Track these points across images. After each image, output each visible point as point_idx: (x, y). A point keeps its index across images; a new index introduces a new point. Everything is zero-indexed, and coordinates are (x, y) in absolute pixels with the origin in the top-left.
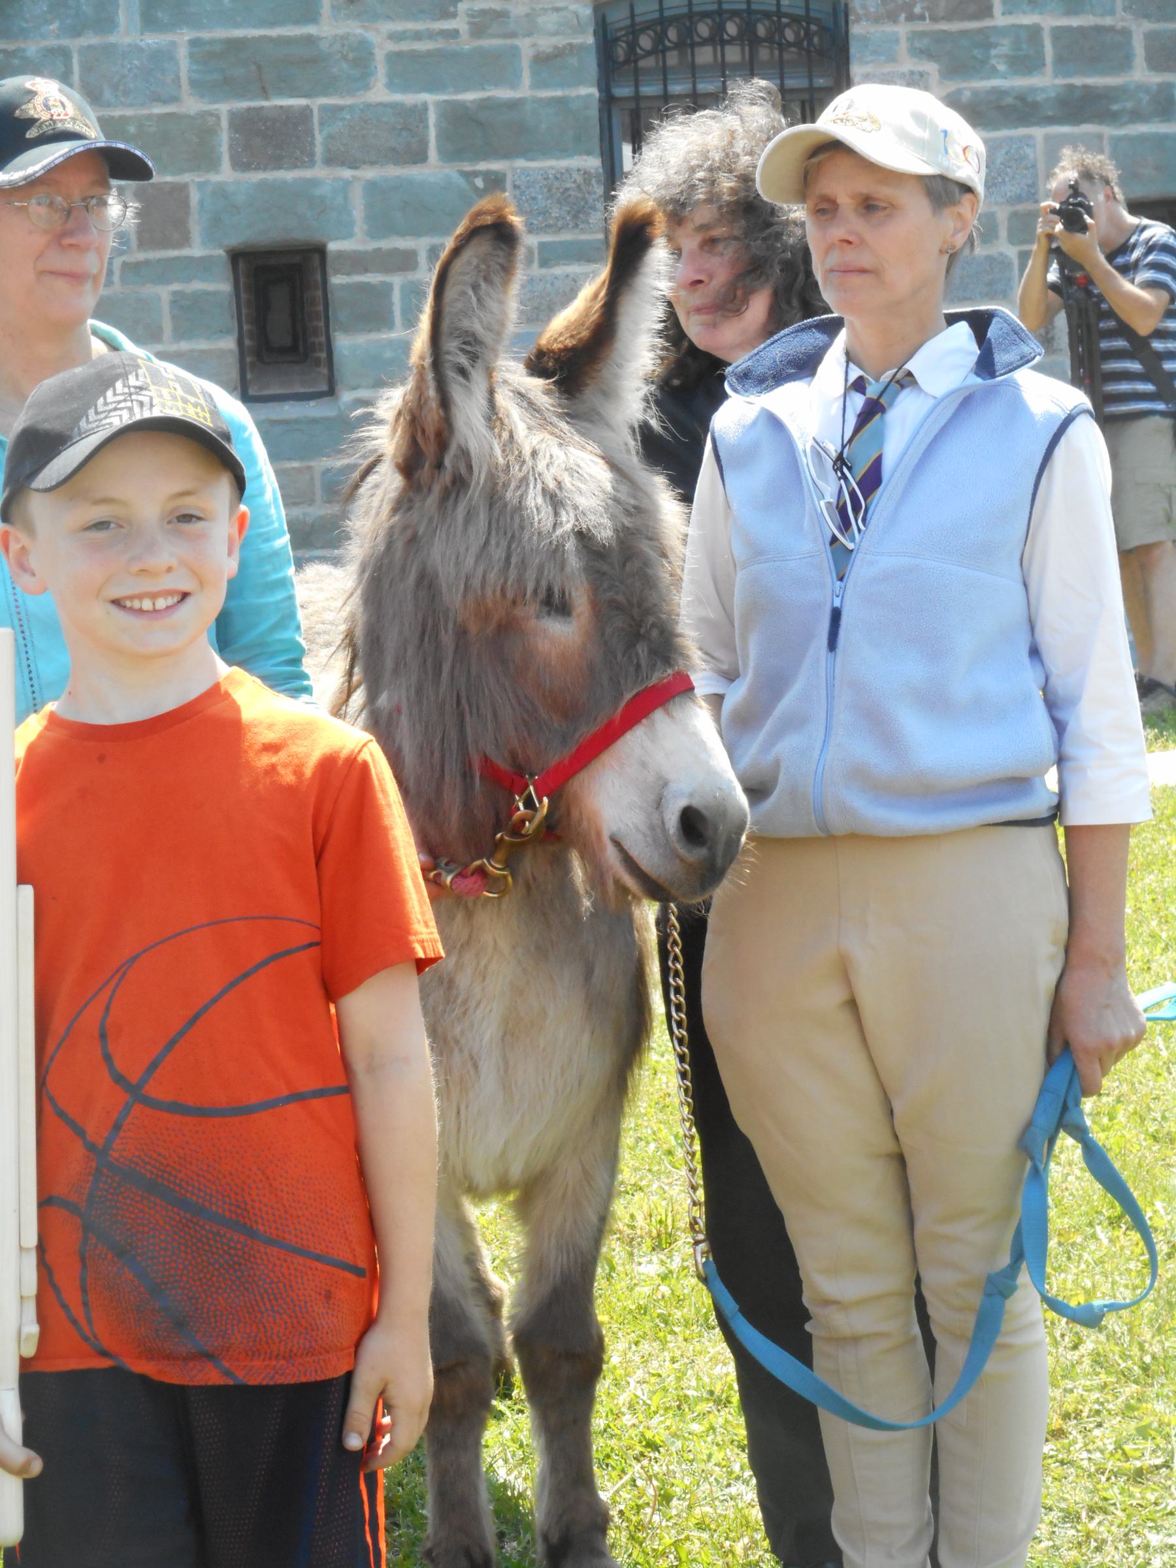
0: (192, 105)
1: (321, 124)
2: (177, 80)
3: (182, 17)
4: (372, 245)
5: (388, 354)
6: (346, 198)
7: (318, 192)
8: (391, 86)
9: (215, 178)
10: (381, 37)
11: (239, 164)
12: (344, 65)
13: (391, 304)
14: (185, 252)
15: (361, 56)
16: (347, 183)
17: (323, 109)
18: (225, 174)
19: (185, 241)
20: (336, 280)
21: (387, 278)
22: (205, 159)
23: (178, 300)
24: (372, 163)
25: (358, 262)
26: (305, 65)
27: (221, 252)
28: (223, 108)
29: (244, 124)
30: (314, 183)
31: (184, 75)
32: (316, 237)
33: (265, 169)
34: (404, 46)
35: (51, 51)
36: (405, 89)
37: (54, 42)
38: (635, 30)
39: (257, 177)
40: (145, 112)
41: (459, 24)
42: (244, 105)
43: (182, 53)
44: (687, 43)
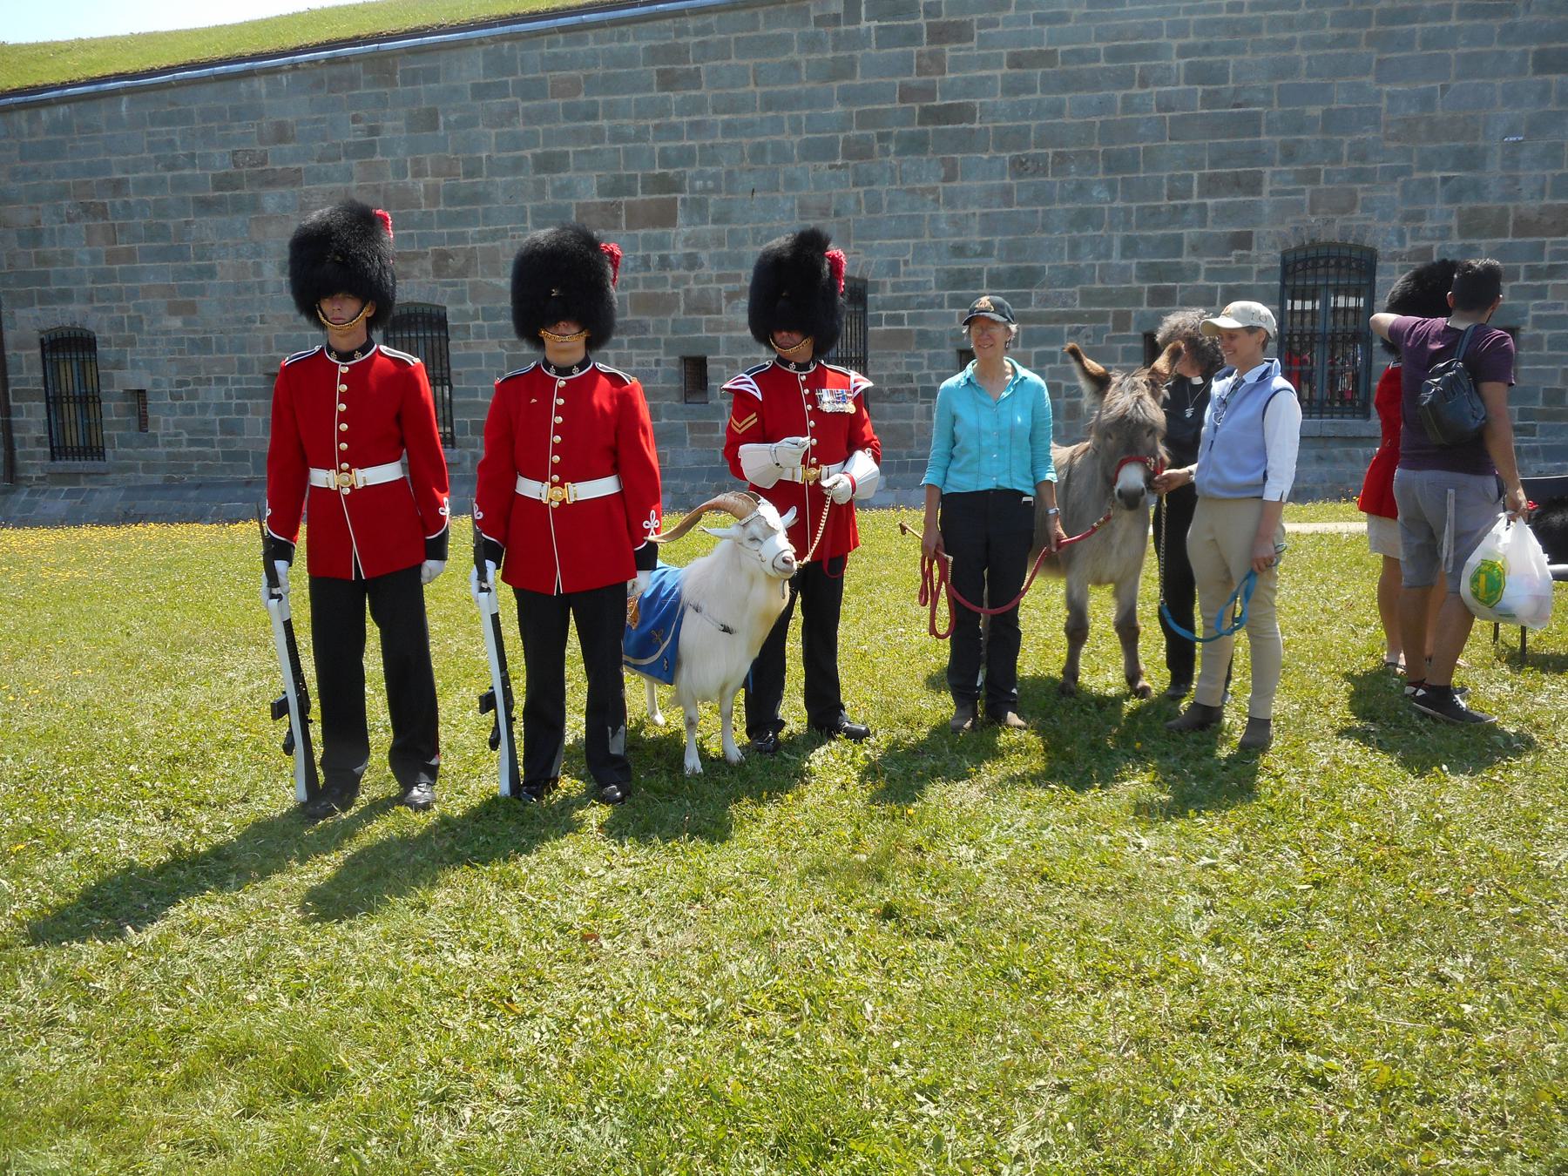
0: (1135, 284)
3: (1135, 254)
8: (1206, 279)
10: (1203, 263)
11: (1150, 304)
15: (1196, 270)
18: (1145, 308)
19: (1128, 329)
22: (1138, 303)
26: (1176, 272)
28: (1146, 286)
29: (1152, 291)
38: (1296, 262)
41: (1232, 259)
44: (1315, 267)
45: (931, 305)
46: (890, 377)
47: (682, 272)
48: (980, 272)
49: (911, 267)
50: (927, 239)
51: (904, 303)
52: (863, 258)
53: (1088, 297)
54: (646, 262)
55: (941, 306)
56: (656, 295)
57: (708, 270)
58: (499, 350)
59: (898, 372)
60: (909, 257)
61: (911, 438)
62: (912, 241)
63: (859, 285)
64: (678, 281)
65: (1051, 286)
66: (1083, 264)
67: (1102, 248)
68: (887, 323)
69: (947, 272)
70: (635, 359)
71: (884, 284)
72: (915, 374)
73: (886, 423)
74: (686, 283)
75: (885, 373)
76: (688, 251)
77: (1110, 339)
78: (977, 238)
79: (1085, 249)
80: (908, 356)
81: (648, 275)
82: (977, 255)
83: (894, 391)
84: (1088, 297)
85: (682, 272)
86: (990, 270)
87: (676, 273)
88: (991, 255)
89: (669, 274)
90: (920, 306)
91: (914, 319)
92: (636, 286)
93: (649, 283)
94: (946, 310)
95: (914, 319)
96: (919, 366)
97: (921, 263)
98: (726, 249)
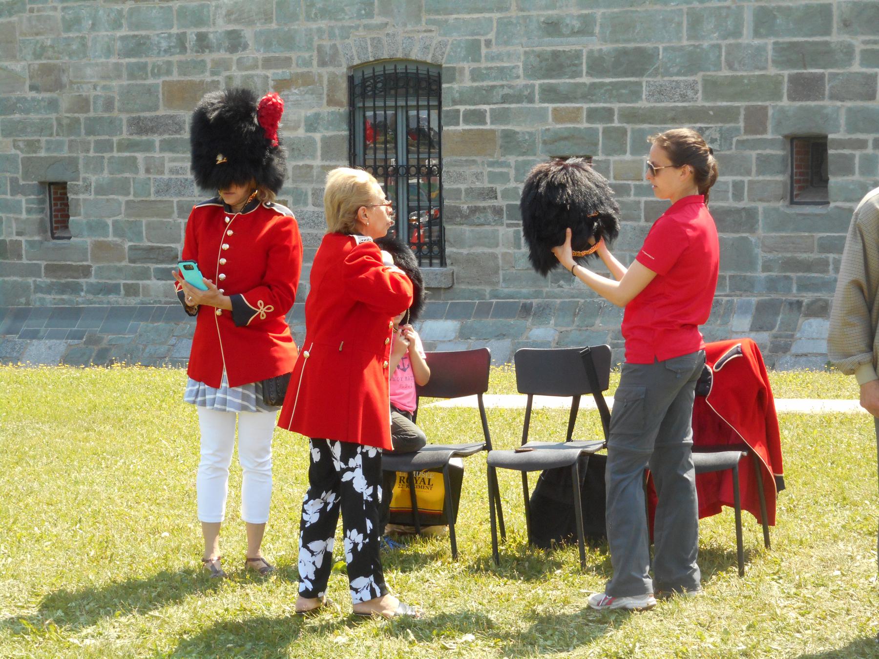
0: (772, 71)
1: (829, 81)
2: (767, 60)
3: (771, 32)
4: (848, 136)
5: (851, 187)
6: (838, 115)
7: (825, 111)
8: (862, 64)
9: (780, 104)
10: (858, 42)
11: (791, 98)
12: (841, 55)
13: (854, 164)
14: (764, 136)
15: (849, 52)
16: (839, 108)
17: (830, 74)
18: (785, 102)
19: (765, 131)
20: (831, 152)
21: (853, 152)
23: (759, 158)
24: (850, 99)
25: (841, 144)
26: (823, 54)
27: (780, 137)
28: (786, 73)
29: (793, 80)
30: (823, 107)
31: (770, 57)
32: (823, 132)
33: (802, 100)
34: (869, 47)
35: (713, 46)
36: (868, 66)
37: (715, 42)
39: (798, 104)
40: (752, 73)
42: (796, 71)
43: (770, 47)
45: (517, 98)
46: (469, 191)
47: (222, 54)
48: (578, 55)
49: (494, 49)
50: (513, 13)
51: (485, 95)
52: (436, 38)
53: (713, 88)
54: (181, 40)
55: (531, 100)
56: (192, 83)
57: (254, 53)
58: (13, 151)
59: (478, 185)
60: (491, 36)
61: (497, 273)
62: (498, 15)
63: (433, 72)
64: (220, 66)
65: (667, 73)
66: (706, 44)
67: (730, 24)
68: (466, 121)
69: (539, 55)
70: (168, 165)
71: (462, 70)
72: (499, 188)
73: (465, 251)
74: (228, 69)
75: (463, 187)
76: (230, 27)
77: (741, 143)
78: (575, 11)
79: (709, 25)
80: (491, 164)
81: (182, 57)
82: (574, 33)
83: (474, 210)
84: (713, 88)
85: (222, 54)
86: (591, 52)
87: (216, 56)
88: (592, 34)
89: (208, 57)
90: (505, 99)
91: (498, 117)
92: (169, 72)
93: (184, 67)
94: (537, 105)
95: (498, 117)
96: (504, 177)
97: (506, 43)
98: (274, 26)
